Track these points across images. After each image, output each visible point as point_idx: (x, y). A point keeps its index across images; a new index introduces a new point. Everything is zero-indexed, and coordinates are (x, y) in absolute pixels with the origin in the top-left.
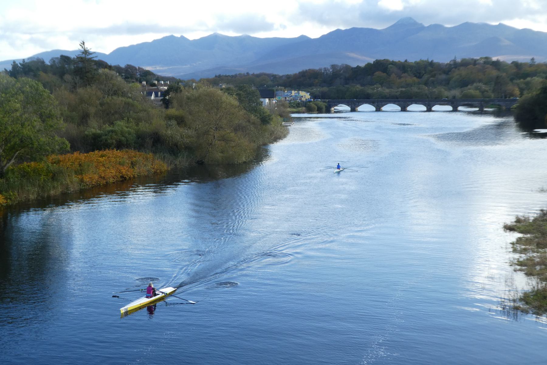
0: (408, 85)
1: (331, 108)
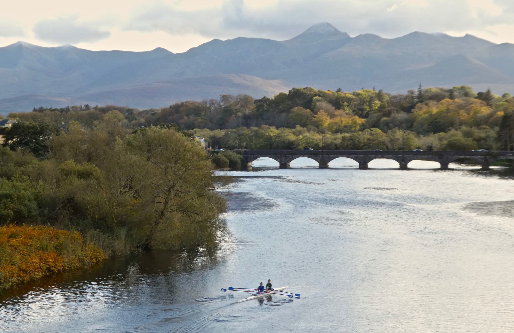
0: (347, 128)
1: (248, 162)
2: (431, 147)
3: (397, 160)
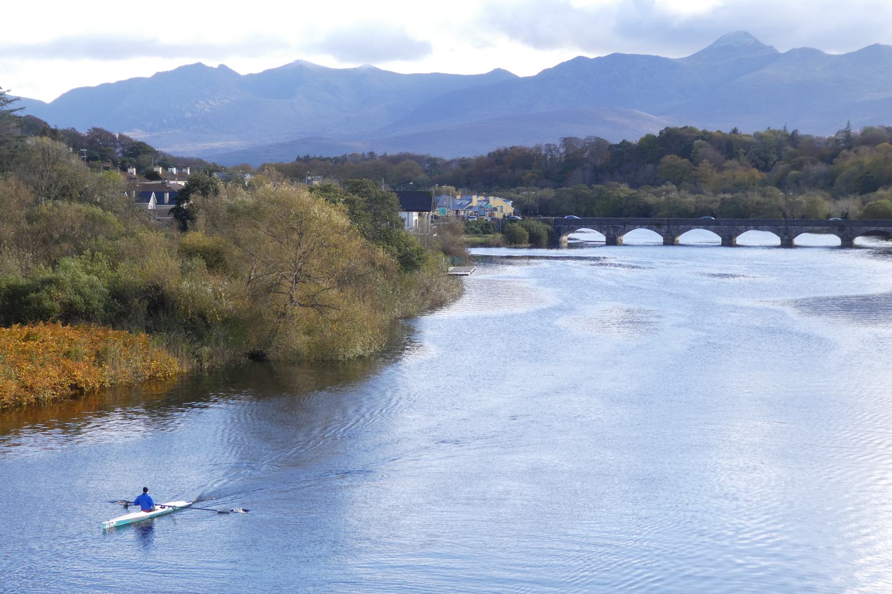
0: (739, 187)
1: (560, 235)
2: (847, 214)
3: (777, 233)
